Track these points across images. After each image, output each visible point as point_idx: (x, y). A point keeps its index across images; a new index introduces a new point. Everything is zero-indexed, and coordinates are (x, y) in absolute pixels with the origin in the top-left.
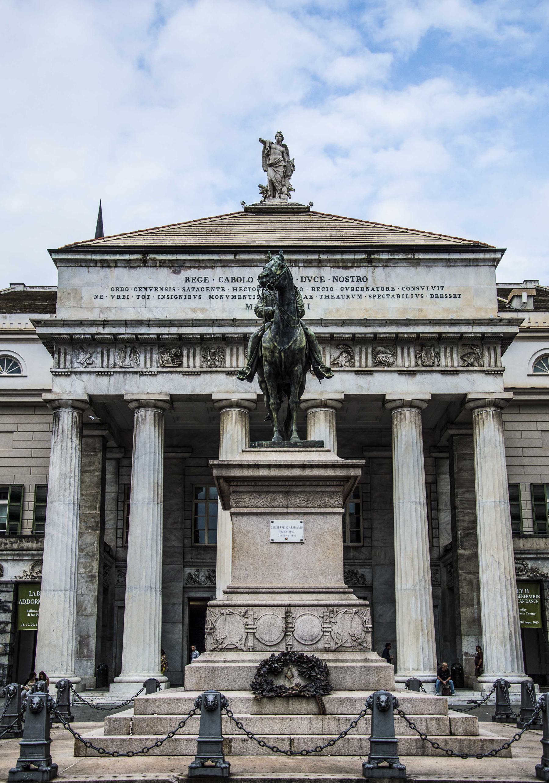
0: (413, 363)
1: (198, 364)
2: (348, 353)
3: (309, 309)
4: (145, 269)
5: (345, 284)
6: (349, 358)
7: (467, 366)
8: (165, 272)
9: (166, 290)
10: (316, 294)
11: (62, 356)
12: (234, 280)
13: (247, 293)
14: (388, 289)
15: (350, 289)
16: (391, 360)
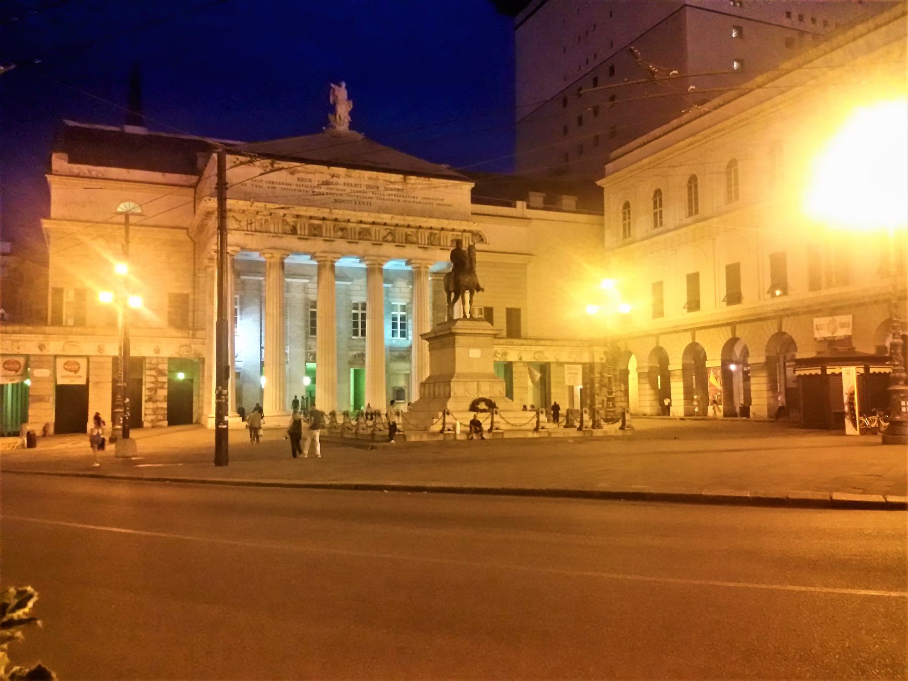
13: (335, 192)
16: (414, 239)
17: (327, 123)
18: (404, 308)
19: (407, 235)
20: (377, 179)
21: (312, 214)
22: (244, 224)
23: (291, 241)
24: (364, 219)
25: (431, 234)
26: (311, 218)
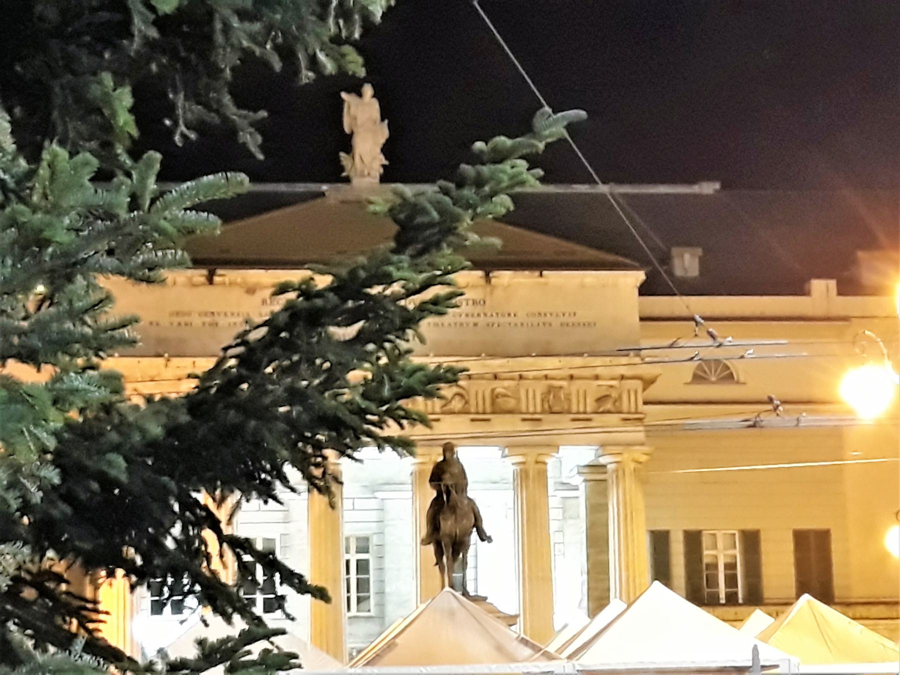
0: (539, 409)
8: (237, 294)
15: (463, 316)
16: (511, 403)
19: (495, 397)
25: (550, 389)
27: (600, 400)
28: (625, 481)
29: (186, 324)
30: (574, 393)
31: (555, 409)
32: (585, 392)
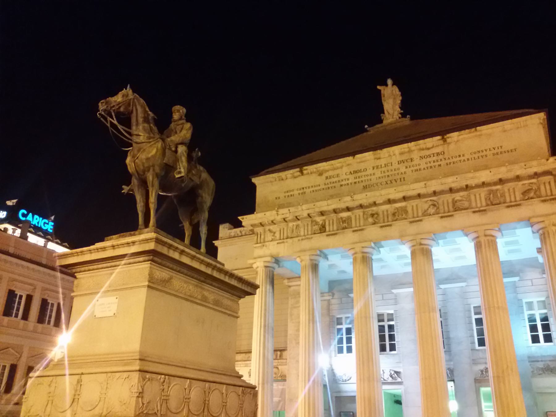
0: (484, 204)
1: (335, 228)
2: (434, 205)
3: (404, 180)
4: (303, 177)
5: (429, 159)
6: (435, 208)
7: (528, 199)
9: (315, 186)
10: (409, 170)
11: (259, 236)
12: (355, 172)
13: (363, 179)
14: (460, 156)
16: (466, 204)
17: (381, 121)
18: (544, 305)
19: (454, 202)
20: (410, 151)
21: (334, 206)
22: (277, 235)
23: (321, 241)
24: (392, 197)
25: (490, 192)
26: (335, 211)
27: (524, 193)
28: (550, 239)
29: (291, 195)
30: (506, 190)
31: (495, 202)
32: (514, 189)
